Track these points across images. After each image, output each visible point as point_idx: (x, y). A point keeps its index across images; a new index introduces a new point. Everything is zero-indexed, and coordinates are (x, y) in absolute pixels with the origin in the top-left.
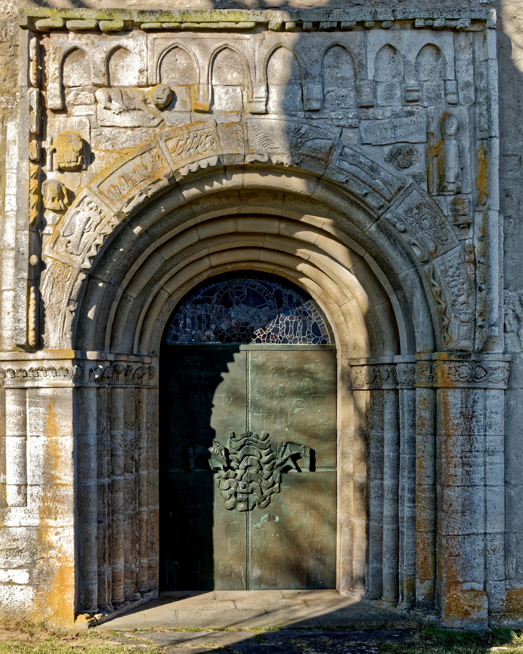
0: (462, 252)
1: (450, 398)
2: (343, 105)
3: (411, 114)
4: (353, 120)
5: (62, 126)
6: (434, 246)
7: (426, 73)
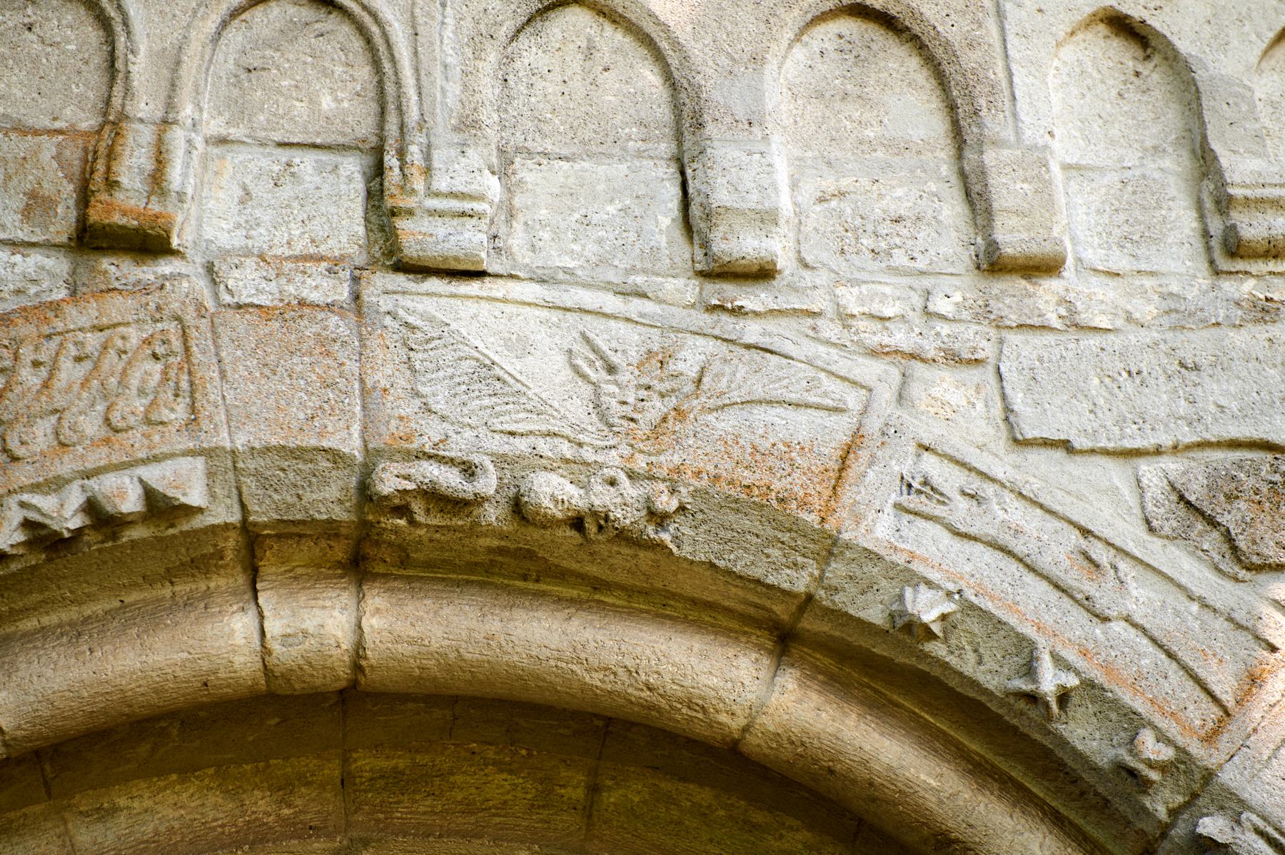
2: (900, 259)
4: (958, 328)
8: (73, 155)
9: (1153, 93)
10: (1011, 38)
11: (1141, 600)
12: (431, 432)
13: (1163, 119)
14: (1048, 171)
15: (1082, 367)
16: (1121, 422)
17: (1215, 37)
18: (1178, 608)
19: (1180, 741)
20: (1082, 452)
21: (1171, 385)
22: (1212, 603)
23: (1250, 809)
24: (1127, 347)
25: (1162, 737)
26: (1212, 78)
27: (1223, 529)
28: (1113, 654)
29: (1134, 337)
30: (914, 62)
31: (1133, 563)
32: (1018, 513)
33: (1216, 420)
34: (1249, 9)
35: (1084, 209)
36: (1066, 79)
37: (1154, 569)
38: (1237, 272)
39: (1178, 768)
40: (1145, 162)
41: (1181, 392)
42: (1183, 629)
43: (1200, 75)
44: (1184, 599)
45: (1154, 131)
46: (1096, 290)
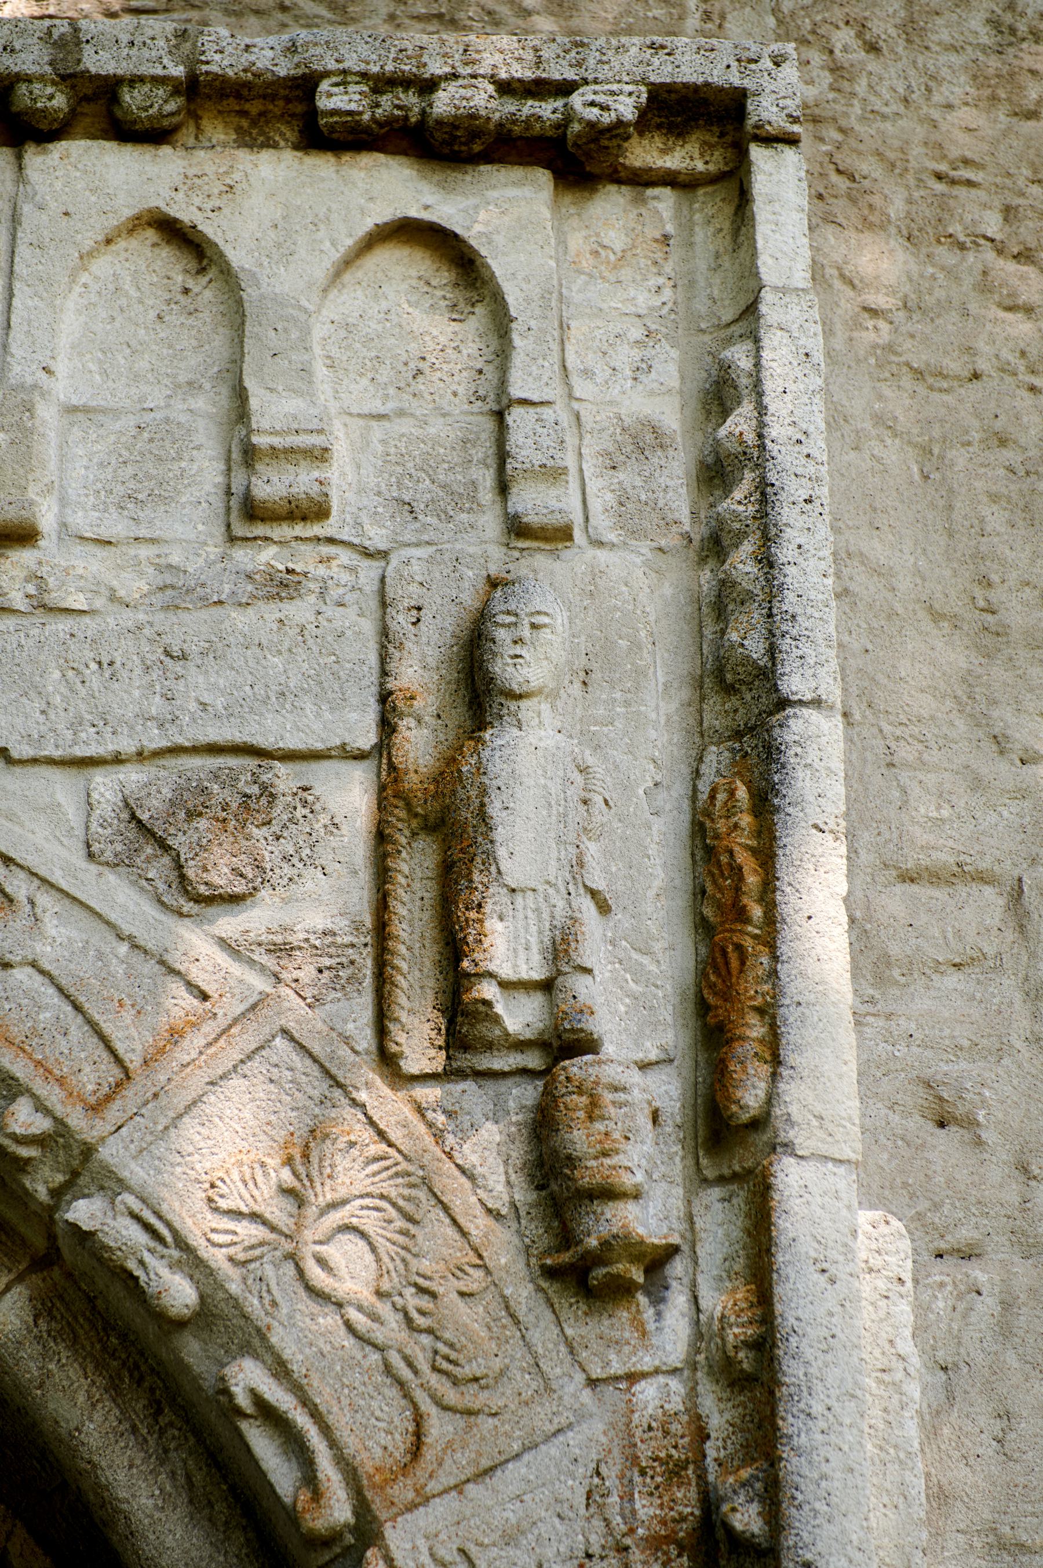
0: (611, 1473)
6: (404, 1423)
7: (385, 374)
9: (201, 315)
10: (22, 250)
11: (59, 940)
13: (207, 347)
14: (32, 417)
15: (42, 658)
16: (77, 725)
17: (278, 245)
18: (103, 950)
19: (59, 1110)
20: (21, 762)
21: (148, 678)
22: (142, 943)
23: (128, 1189)
24: (101, 633)
25: (41, 1107)
26: (262, 297)
27: (174, 853)
28: (7, 1007)
29: (115, 619)
31: (59, 896)
33: (194, 720)
34: (329, 210)
35: (85, 462)
36: (94, 298)
37: (81, 903)
38: (255, 538)
39: (56, 1142)
40: (172, 402)
41: (158, 687)
42: (103, 975)
43: (249, 294)
44: (111, 937)
45: (193, 362)
46: (76, 563)
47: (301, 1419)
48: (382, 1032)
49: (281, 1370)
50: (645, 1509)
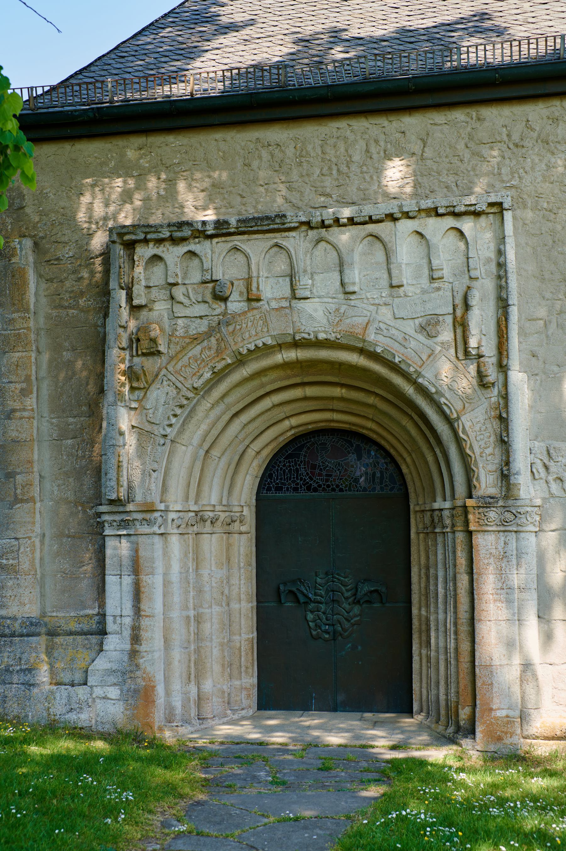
1: (480, 540)
2: (377, 287)
3: (438, 289)
5: (145, 319)
6: (462, 405)
8: (245, 283)
12: (303, 328)
16: (412, 313)
30: (381, 245)
32: (394, 331)
43: (430, 243)
47: (450, 405)
48: (456, 354)
49: (447, 399)
50: (493, 413)
